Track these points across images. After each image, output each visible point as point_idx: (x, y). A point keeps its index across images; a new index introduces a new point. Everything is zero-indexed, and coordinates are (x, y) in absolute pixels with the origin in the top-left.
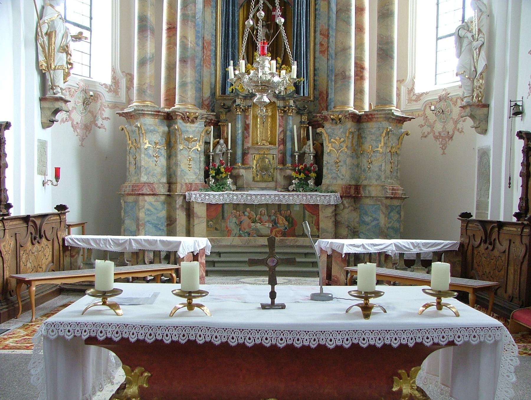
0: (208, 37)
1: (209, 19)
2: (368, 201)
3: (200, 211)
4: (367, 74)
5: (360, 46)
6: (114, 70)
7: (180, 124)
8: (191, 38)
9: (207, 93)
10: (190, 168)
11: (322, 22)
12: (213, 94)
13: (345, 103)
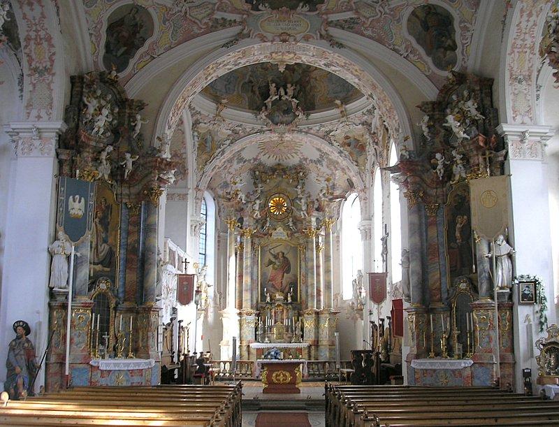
0: (255, 278)
1: (255, 270)
2: (322, 347)
3: (254, 352)
4: (322, 293)
5: (318, 282)
6: (215, 292)
7: (245, 317)
8: (249, 280)
9: (255, 302)
10: (251, 336)
11: (303, 271)
12: (257, 302)
13: (313, 307)
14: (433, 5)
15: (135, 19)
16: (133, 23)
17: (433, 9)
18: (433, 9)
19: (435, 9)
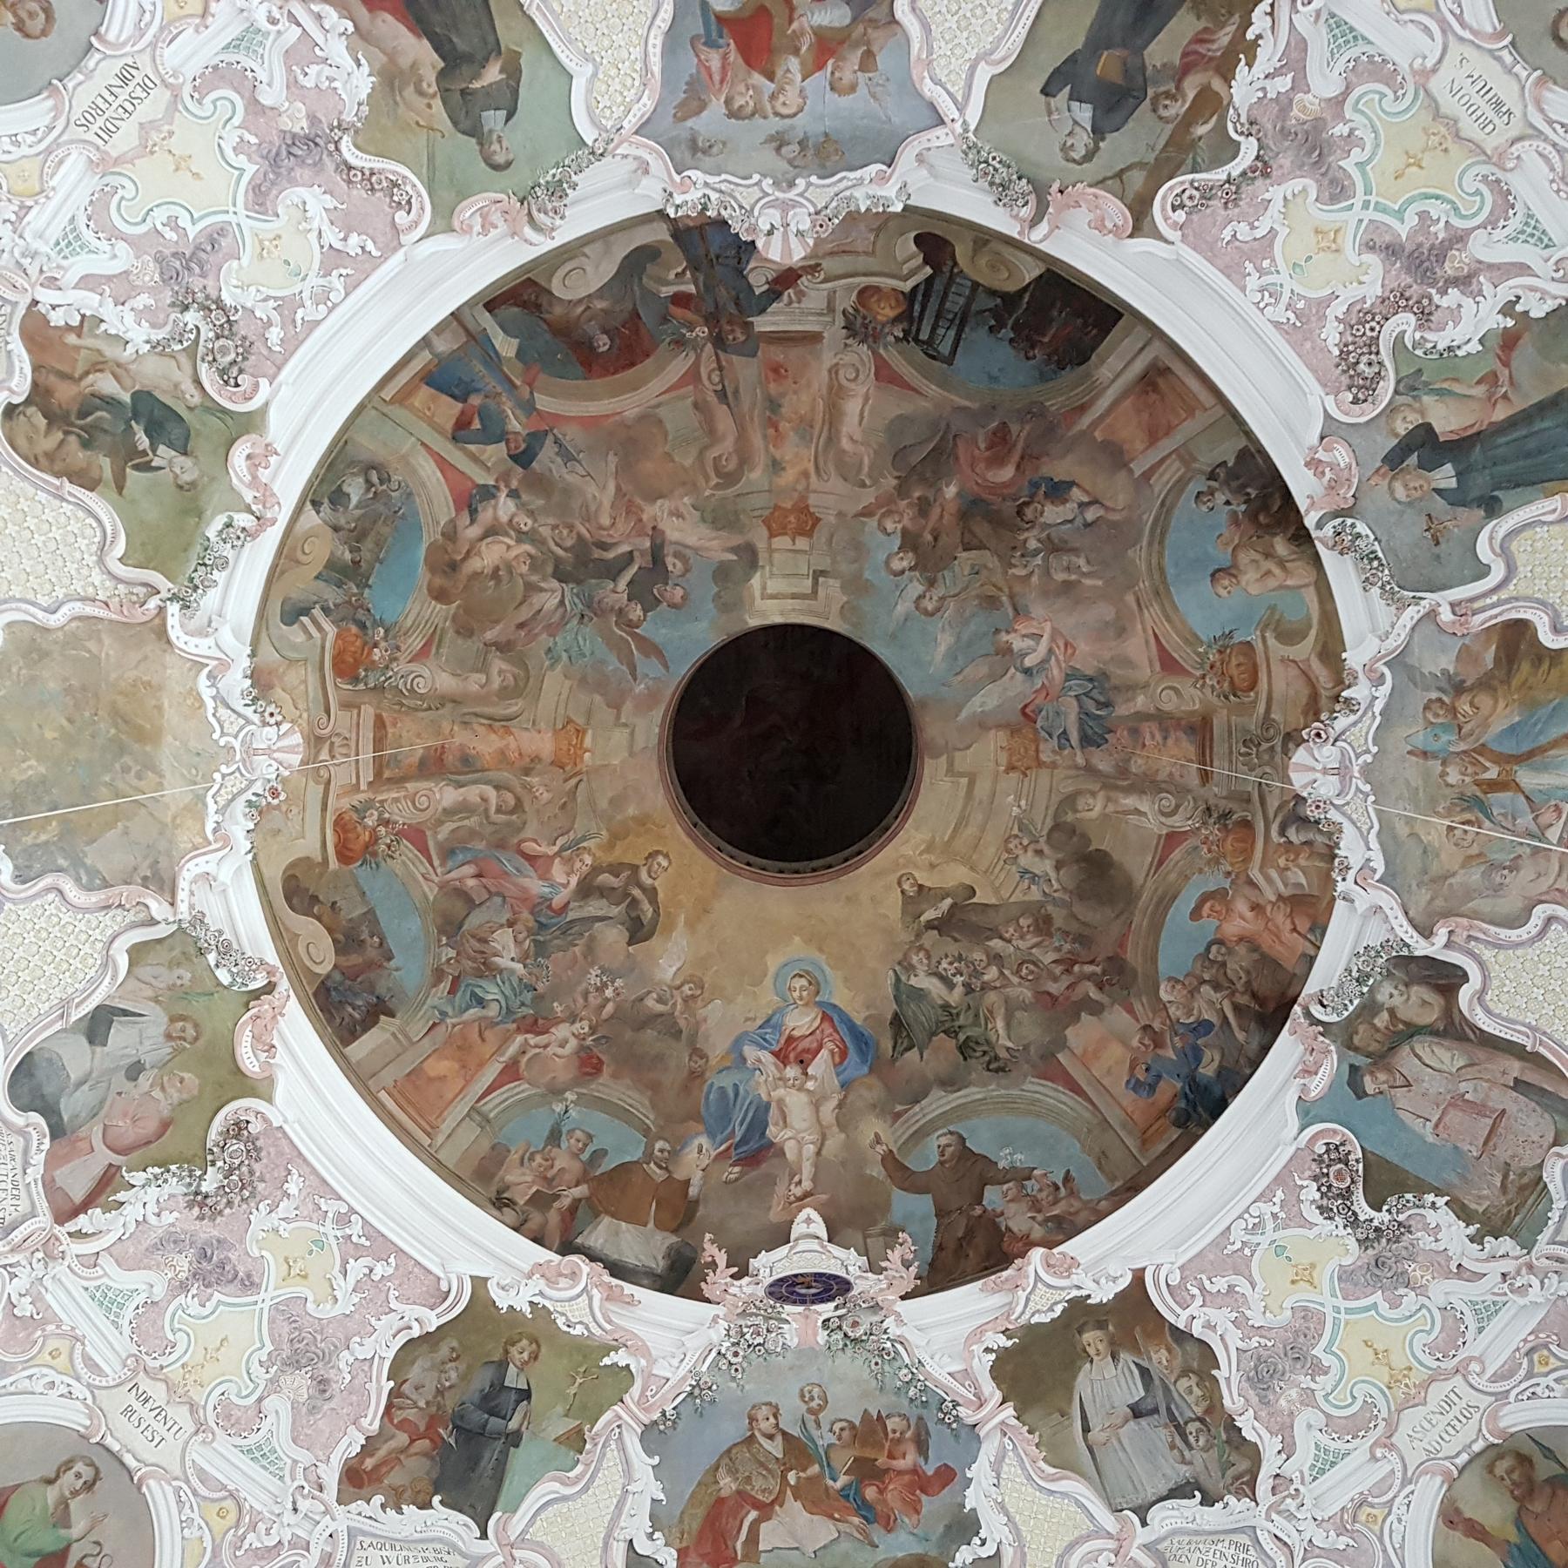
14: (1530, 1435)
15: (62, 1517)
16: (47, 1541)
17: (1537, 1457)
18: (1537, 1457)
19: (1548, 1453)
